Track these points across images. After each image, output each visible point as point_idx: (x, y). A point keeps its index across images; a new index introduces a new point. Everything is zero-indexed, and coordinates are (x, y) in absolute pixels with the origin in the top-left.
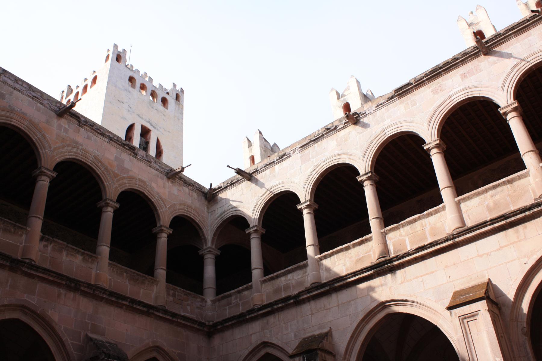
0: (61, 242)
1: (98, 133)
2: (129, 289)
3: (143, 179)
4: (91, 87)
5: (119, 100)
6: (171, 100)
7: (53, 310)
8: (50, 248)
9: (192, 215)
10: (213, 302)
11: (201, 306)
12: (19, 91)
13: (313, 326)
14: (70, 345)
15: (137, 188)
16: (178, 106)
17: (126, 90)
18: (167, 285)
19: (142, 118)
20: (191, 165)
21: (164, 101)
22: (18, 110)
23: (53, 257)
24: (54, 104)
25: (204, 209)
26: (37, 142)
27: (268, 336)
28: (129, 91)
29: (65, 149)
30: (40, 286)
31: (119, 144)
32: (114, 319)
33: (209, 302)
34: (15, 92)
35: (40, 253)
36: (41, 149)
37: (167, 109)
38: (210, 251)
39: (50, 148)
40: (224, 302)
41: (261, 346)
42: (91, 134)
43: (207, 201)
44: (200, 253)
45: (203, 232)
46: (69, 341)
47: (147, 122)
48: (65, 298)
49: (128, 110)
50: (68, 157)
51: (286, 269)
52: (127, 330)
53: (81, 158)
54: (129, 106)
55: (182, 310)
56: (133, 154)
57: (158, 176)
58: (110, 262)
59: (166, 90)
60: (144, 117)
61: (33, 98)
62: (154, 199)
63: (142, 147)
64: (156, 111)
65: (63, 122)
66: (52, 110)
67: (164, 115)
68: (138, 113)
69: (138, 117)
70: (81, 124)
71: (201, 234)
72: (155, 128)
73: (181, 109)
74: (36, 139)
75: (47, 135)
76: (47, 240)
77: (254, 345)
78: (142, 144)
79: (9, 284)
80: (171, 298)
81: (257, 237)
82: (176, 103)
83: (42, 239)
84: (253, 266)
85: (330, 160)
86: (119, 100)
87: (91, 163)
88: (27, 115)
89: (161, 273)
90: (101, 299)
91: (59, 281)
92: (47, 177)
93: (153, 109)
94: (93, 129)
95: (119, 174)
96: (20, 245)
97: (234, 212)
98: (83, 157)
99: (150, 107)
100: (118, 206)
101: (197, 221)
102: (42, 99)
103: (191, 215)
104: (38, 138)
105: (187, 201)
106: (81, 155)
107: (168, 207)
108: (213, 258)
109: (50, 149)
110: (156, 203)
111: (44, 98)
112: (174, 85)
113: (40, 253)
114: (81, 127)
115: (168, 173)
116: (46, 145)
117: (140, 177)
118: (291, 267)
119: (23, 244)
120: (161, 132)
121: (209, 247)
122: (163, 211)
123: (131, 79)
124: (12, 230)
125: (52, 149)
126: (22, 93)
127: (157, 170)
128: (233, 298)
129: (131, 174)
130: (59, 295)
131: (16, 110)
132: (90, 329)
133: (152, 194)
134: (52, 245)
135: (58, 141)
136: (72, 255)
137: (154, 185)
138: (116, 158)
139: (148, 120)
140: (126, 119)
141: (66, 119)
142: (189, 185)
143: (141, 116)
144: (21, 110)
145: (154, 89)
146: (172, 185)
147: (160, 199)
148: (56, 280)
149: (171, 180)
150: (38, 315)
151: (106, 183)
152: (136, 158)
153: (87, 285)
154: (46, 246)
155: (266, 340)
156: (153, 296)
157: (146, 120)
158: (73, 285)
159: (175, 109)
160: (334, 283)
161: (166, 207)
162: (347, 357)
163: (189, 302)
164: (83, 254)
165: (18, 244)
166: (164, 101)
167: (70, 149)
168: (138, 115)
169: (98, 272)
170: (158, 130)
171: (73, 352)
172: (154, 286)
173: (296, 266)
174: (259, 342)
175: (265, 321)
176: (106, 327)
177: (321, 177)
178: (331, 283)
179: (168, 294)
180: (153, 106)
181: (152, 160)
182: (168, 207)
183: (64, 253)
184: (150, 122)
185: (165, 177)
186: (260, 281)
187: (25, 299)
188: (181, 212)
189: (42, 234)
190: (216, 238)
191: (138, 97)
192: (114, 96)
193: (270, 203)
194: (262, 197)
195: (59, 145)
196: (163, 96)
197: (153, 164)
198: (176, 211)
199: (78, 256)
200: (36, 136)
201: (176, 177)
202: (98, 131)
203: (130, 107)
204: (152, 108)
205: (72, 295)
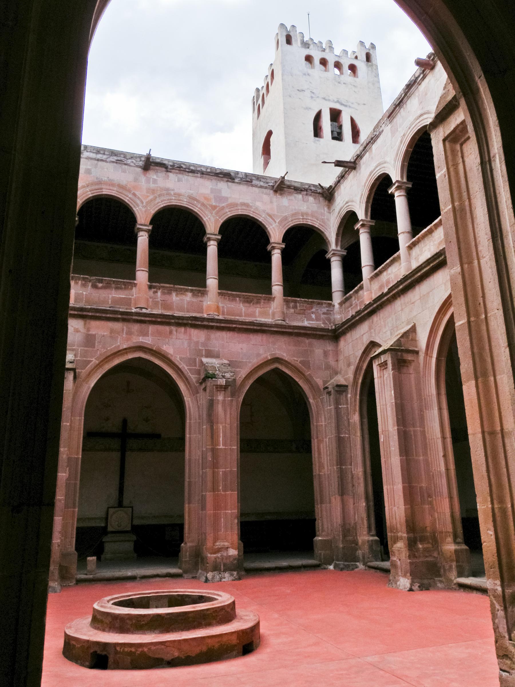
0: (168, 285)
1: (188, 172)
2: (243, 311)
3: (246, 201)
4: (271, 84)
5: (298, 90)
6: (361, 65)
8: (159, 293)
9: (309, 221)
10: (341, 304)
11: (329, 311)
12: (102, 160)
13: (403, 323)
15: (240, 213)
16: (370, 68)
17: (305, 74)
18: (284, 299)
19: (329, 100)
20: (287, 172)
21: (353, 68)
22: (106, 178)
23: (163, 300)
24: (138, 160)
25: (324, 211)
26: (130, 202)
27: (374, 335)
28: (308, 74)
29: (158, 200)
30: (152, 328)
31: (212, 176)
32: (227, 342)
33: (337, 306)
34: (100, 163)
35: (151, 300)
36: (134, 206)
37: (357, 77)
38: (333, 254)
39: (142, 203)
40: (347, 304)
41: (371, 346)
42: (180, 176)
43: (327, 201)
44: (327, 257)
45: (325, 235)
46: (186, 368)
47: (336, 102)
48: (177, 333)
49: (312, 97)
50: (162, 206)
51: (385, 263)
52: (241, 349)
53: (174, 202)
54: (311, 92)
55: (306, 319)
56: (230, 180)
57: (263, 193)
58: (220, 291)
59: (354, 52)
60: (331, 98)
62: (261, 218)
63: (336, 133)
64: (344, 85)
65: (152, 175)
66: (137, 166)
67: (354, 86)
68: (323, 97)
69: (324, 100)
71: (325, 238)
72: (346, 106)
73: (375, 71)
76: (155, 287)
77: (365, 346)
78: (335, 130)
79: (125, 332)
80: (292, 310)
81: (365, 232)
82: (367, 65)
83: (150, 287)
84: (363, 264)
85: (414, 125)
86: (299, 89)
87: (186, 204)
88: (114, 181)
89: (277, 289)
90: (212, 328)
92: (144, 232)
93: (340, 85)
95: (218, 205)
96: (132, 297)
97: (347, 208)
99: (336, 83)
100: (219, 237)
101: (317, 226)
102: (126, 159)
103: (308, 222)
104: (130, 198)
105: (301, 208)
107: (277, 221)
108: (338, 260)
109: (143, 204)
110: (264, 221)
111: (128, 158)
112: (362, 43)
113: (151, 300)
114: (170, 172)
115: (273, 186)
116: (138, 202)
117: (241, 201)
118: (388, 261)
119: (135, 296)
120: (354, 108)
121: (333, 250)
122: (273, 228)
123: (309, 59)
124: (123, 286)
125: (144, 204)
126: (105, 161)
127: (261, 187)
128: (353, 298)
129: (230, 201)
130: (171, 332)
131: (104, 180)
132: (204, 354)
133: (258, 214)
134: (161, 290)
135: (149, 194)
136: (181, 294)
137: (258, 204)
138: (212, 191)
139: (336, 100)
140: (310, 108)
141: (153, 169)
142: (302, 191)
143: (327, 98)
144: (108, 178)
145: (337, 59)
146: (280, 197)
147: (268, 217)
149: (279, 192)
150: (155, 351)
151: (205, 218)
152: (234, 182)
154: (156, 292)
155: (372, 340)
156: (271, 312)
157: (334, 100)
159: (368, 73)
161: (275, 222)
162: (429, 353)
163: (314, 310)
164: (192, 291)
165: (130, 297)
166: (353, 68)
167: (162, 198)
168: (324, 99)
169: (209, 303)
170: (350, 107)
171: (191, 375)
172: (271, 303)
173: (391, 258)
174: (368, 342)
175: (371, 321)
176: (220, 350)
177: (411, 148)
179: (288, 307)
180: (339, 81)
181: (254, 178)
182: (277, 221)
183: (174, 294)
184: (340, 101)
185: (272, 192)
186: (368, 279)
187: (141, 340)
188: (294, 222)
189: (149, 283)
190: (340, 238)
191: (320, 77)
192: (293, 87)
193: (374, 190)
194: (365, 186)
195: (151, 197)
196: (349, 63)
197: (255, 182)
198: (289, 223)
199: (187, 293)
200: (127, 196)
201: (284, 188)
202: (187, 170)
203: (313, 93)
204: (339, 83)
205: (182, 329)
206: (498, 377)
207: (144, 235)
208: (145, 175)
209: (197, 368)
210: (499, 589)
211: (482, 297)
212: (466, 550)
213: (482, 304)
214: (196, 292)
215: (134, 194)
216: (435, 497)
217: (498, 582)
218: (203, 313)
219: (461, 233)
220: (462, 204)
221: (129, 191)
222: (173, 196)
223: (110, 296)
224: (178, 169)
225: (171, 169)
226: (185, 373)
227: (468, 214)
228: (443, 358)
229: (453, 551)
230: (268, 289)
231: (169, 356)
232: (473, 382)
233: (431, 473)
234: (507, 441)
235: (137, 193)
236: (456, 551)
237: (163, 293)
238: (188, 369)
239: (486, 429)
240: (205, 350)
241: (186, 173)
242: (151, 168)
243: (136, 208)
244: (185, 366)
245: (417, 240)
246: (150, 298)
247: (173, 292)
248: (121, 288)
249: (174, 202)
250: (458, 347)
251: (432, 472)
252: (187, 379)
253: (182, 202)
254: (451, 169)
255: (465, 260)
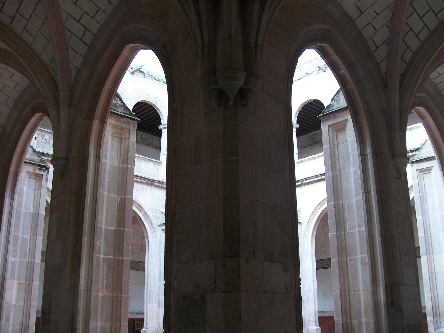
7: (141, 197)
14: (152, 216)
46: (151, 214)
48: (146, 190)
70: (145, 76)
91: (143, 181)
94: (152, 78)
114: (145, 78)
130: (143, 189)
132: (161, 206)
148: (141, 180)
153: (158, 182)
158: (150, 182)
160: (304, 181)
162: (308, 225)
171: (153, 220)
178: (302, 180)
206: (434, 256)
209: (157, 215)
210: (432, 319)
211: (430, 229)
212: (320, 329)
213: (429, 231)
214: (156, 163)
216: (306, 302)
217: (432, 317)
218: (159, 178)
219: (422, 205)
220: (423, 195)
226: (150, 217)
227: (425, 199)
228: (315, 229)
229: (315, 329)
230: (158, 157)
231: (142, 205)
232: (426, 256)
233: (305, 290)
234: (436, 275)
236: (316, 329)
238: (152, 215)
239: (430, 271)
240: (162, 203)
244: (151, 213)
245: (304, 160)
247: (142, 160)
250: (420, 244)
251: (305, 289)
252: (151, 222)
254: (419, 181)
255: (424, 215)
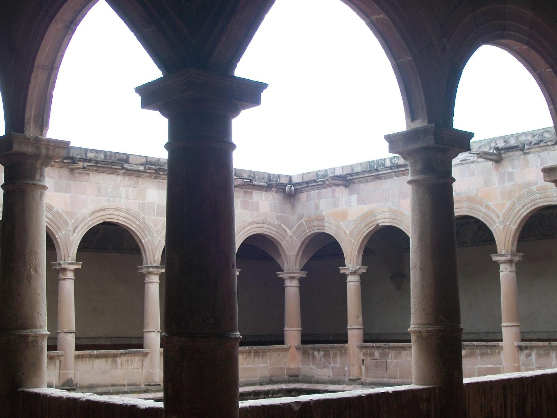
8: (534, 356)
39: (498, 217)
53: (541, 203)
61: (462, 164)
70: (525, 151)
74: (482, 217)
75: (491, 203)
76: (526, 348)
98: (544, 199)
104: (484, 213)
106: (540, 199)
114: (529, 153)
116: (494, 217)
125: (501, 217)
134: (535, 351)
141: (506, 157)
154: (529, 355)
165: (498, 366)
195: (508, 204)
200: (481, 212)
207: (504, 269)
208: (497, 169)
215: (487, 207)
221: (481, 203)
222: (536, 193)
223: (476, 367)
224: (537, 146)
225: (528, 149)
235: (490, 204)
237: (539, 356)
241: (551, 147)
242: (504, 157)
243: (493, 227)
246: (523, 365)
248: (487, 354)
249: (541, 203)
253: (551, 199)
